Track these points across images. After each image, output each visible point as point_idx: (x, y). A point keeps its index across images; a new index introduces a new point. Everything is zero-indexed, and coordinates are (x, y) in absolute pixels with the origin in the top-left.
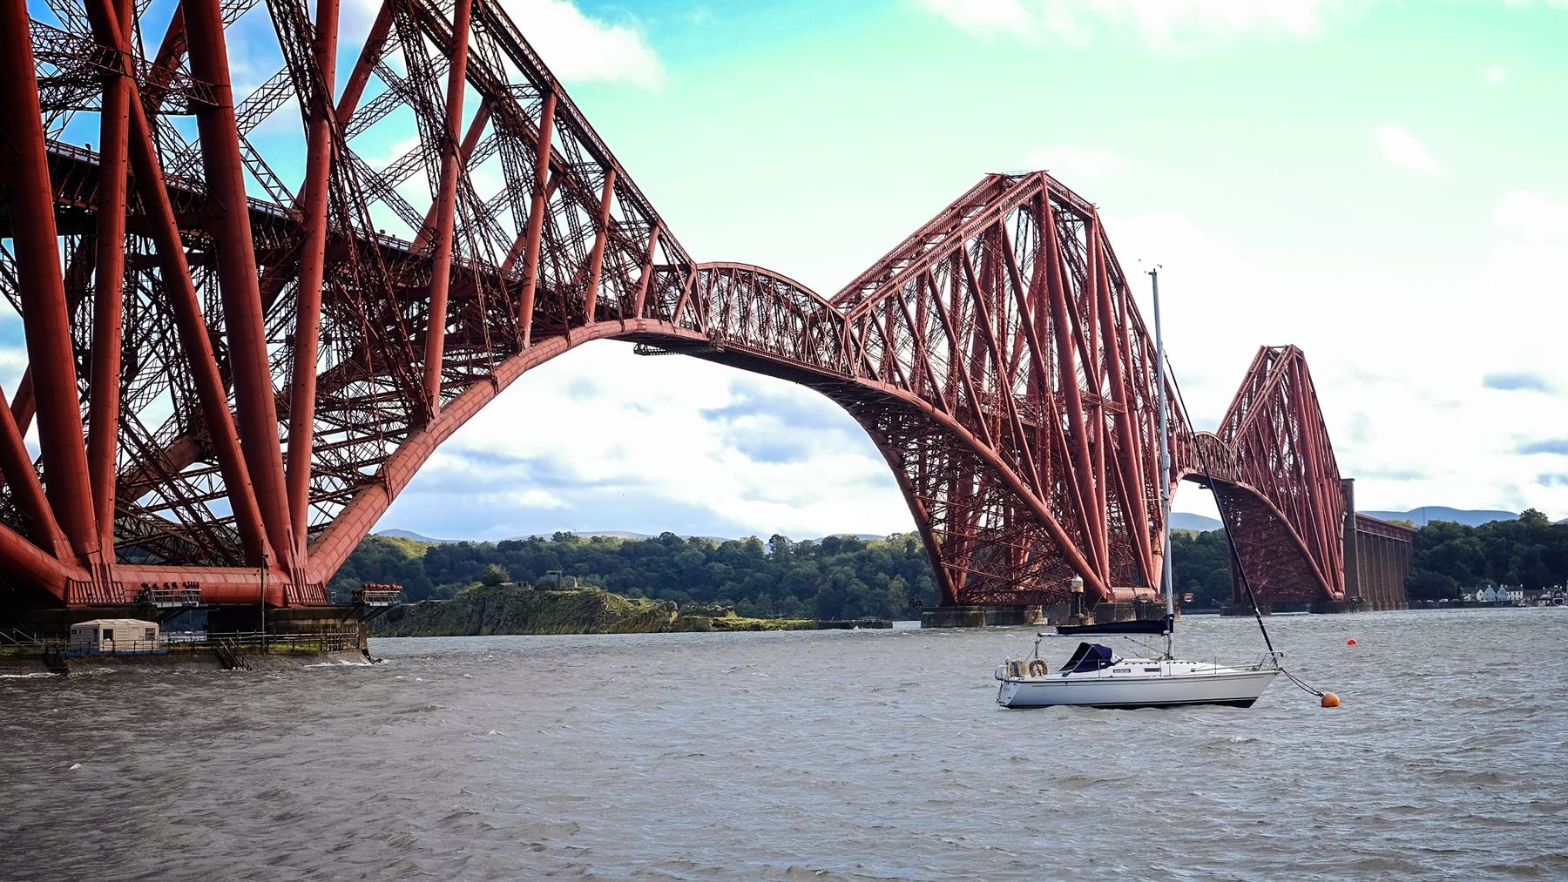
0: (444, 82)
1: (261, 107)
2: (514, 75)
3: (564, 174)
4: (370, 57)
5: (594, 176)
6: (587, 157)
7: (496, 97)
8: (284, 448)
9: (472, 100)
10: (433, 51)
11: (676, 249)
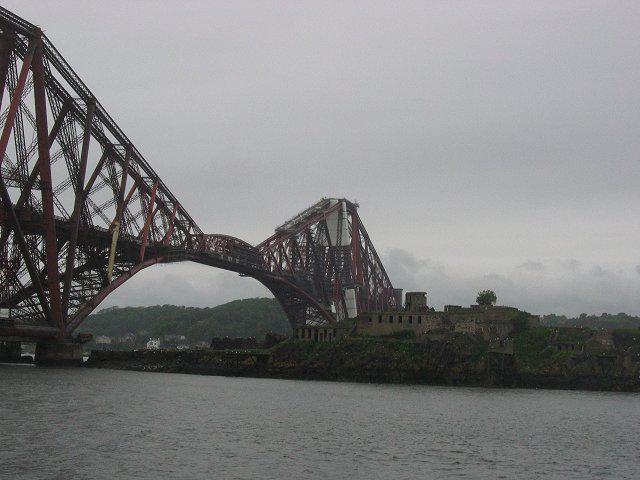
0: (120, 180)
1: (62, 187)
2: (143, 174)
3: (162, 205)
4: (98, 171)
5: (170, 207)
6: (167, 199)
7: (139, 182)
8: (62, 290)
9: (130, 182)
10: (118, 168)
11: (198, 229)
